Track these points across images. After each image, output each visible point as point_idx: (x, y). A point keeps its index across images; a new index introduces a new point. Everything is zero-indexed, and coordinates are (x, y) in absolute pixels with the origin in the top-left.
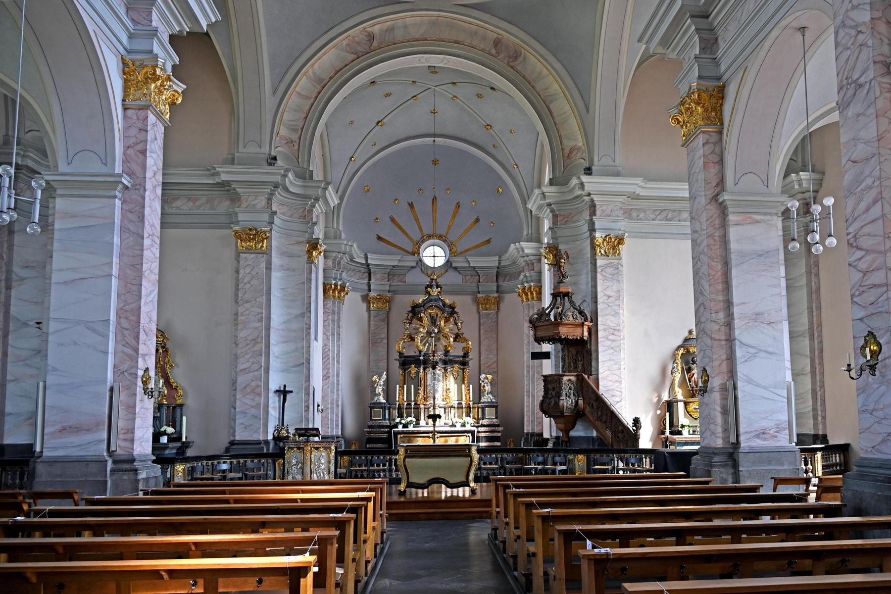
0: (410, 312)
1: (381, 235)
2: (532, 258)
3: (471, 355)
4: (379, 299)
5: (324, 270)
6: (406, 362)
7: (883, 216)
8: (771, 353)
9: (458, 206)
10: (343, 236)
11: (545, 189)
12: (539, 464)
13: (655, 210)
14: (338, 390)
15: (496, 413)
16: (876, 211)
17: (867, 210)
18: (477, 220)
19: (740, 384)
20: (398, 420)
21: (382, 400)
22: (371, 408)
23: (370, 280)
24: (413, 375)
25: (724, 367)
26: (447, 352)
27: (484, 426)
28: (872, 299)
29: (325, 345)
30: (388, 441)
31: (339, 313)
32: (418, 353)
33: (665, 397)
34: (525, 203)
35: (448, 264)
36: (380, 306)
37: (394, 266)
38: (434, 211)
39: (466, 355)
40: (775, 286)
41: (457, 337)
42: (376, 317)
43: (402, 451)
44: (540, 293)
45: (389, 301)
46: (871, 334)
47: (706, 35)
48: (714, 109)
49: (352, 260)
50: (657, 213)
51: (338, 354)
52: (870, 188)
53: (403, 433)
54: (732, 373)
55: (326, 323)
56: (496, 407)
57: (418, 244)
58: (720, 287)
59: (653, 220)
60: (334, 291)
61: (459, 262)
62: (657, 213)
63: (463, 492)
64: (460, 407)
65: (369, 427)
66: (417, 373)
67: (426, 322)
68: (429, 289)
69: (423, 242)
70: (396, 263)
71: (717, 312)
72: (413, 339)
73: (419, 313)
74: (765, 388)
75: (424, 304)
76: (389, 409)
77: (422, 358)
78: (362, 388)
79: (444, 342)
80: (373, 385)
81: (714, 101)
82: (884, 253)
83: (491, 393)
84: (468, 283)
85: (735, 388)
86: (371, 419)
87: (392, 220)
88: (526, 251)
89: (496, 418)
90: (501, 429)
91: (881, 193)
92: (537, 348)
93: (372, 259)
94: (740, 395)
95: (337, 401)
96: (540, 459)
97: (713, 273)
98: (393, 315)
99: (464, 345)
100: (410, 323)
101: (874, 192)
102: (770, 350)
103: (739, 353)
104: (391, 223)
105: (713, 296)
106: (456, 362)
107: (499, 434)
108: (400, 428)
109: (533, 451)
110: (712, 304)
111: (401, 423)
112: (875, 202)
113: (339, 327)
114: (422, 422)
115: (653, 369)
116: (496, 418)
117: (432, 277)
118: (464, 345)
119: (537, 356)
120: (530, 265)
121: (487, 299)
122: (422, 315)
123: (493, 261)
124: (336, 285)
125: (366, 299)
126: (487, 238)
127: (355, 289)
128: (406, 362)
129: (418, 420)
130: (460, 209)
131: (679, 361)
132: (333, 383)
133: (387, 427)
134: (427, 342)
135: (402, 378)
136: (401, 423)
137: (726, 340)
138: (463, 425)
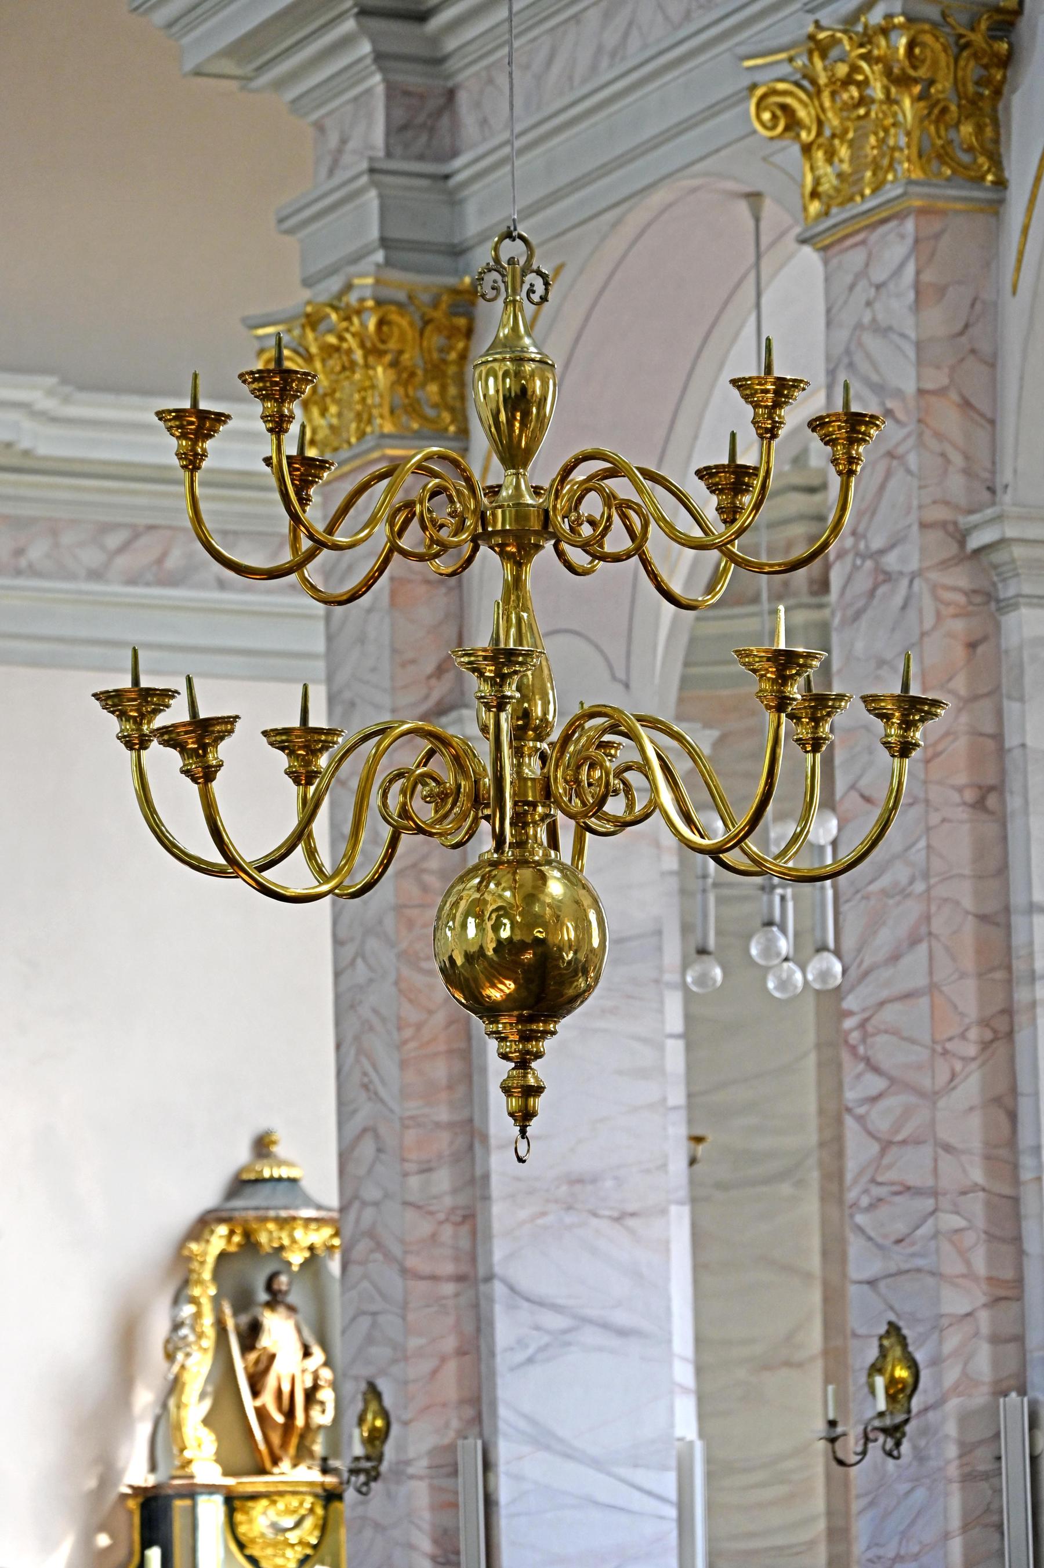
7: (933, 988)
8: (623, 1333)
13: (106, 528)
16: (913, 970)
17: (895, 958)
19: (504, 1451)
25: (449, 1386)
28: (900, 1228)
33: (136, 1473)
40: (642, 1073)
46: (894, 1329)
47: (413, 79)
48: (436, 371)
50: (113, 541)
52: (904, 893)
54: (478, 1408)
58: (440, 1071)
59: (95, 575)
62: (113, 541)
71: (426, 1169)
74: (596, 1464)
81: (435, 340)
82: (932, 1097)
85: (488, 1466)
91: (928, 918)
94: (504, 1494)
97: (413, 1015)
101: (913, 909)
102: (621, 1318)
103: (507, 1329)
105: (413, 1107)
110: (411, 1136)
112: (914, 941)
115: (72, 1329)
131: (206, 1291)
137: (460, 1278)
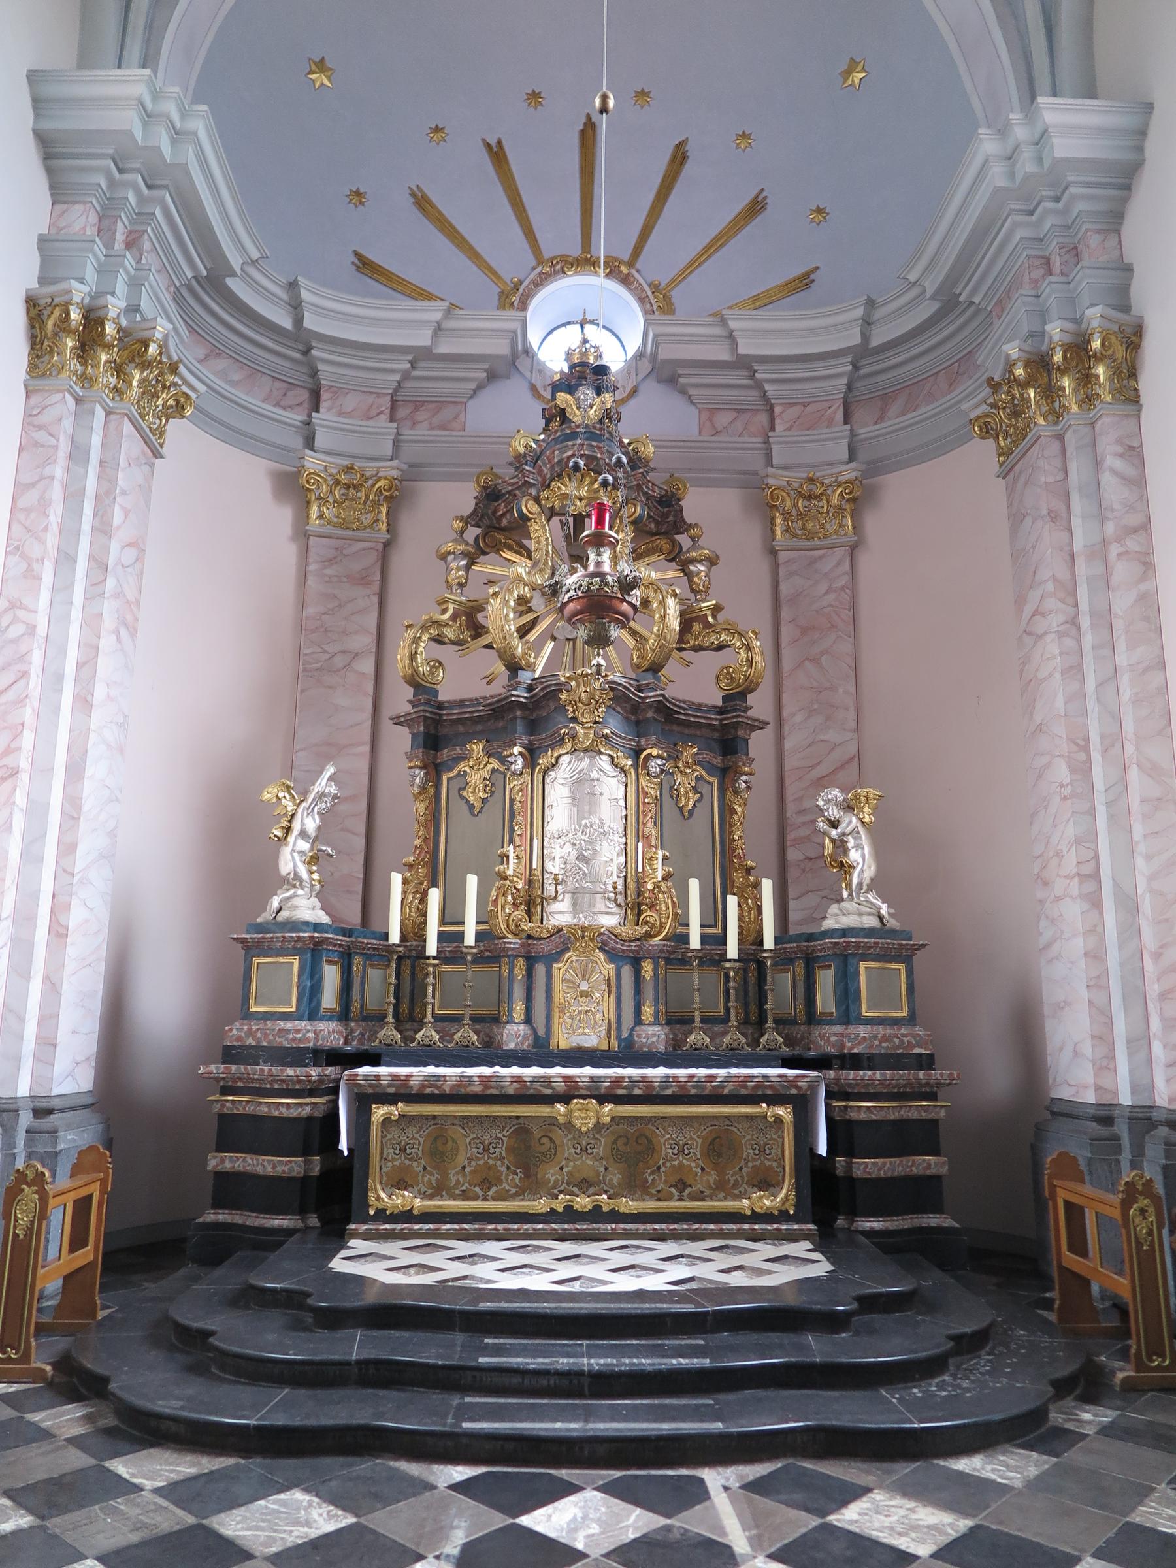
6: (439, 733)
9: (679, 157)
18: (756, 207)
36: (350, 522)
37: (420, 356)
39: (736, 698)
42: (331, 561)
51: (87, 664)
55: (30, 499)
70: (423, 339)
83: (875, 885)
87: (422, 202)
93: (320, 311)
125: (293, 487)
128: (439, 733)
130: (689, 169)
132: (37, 811)
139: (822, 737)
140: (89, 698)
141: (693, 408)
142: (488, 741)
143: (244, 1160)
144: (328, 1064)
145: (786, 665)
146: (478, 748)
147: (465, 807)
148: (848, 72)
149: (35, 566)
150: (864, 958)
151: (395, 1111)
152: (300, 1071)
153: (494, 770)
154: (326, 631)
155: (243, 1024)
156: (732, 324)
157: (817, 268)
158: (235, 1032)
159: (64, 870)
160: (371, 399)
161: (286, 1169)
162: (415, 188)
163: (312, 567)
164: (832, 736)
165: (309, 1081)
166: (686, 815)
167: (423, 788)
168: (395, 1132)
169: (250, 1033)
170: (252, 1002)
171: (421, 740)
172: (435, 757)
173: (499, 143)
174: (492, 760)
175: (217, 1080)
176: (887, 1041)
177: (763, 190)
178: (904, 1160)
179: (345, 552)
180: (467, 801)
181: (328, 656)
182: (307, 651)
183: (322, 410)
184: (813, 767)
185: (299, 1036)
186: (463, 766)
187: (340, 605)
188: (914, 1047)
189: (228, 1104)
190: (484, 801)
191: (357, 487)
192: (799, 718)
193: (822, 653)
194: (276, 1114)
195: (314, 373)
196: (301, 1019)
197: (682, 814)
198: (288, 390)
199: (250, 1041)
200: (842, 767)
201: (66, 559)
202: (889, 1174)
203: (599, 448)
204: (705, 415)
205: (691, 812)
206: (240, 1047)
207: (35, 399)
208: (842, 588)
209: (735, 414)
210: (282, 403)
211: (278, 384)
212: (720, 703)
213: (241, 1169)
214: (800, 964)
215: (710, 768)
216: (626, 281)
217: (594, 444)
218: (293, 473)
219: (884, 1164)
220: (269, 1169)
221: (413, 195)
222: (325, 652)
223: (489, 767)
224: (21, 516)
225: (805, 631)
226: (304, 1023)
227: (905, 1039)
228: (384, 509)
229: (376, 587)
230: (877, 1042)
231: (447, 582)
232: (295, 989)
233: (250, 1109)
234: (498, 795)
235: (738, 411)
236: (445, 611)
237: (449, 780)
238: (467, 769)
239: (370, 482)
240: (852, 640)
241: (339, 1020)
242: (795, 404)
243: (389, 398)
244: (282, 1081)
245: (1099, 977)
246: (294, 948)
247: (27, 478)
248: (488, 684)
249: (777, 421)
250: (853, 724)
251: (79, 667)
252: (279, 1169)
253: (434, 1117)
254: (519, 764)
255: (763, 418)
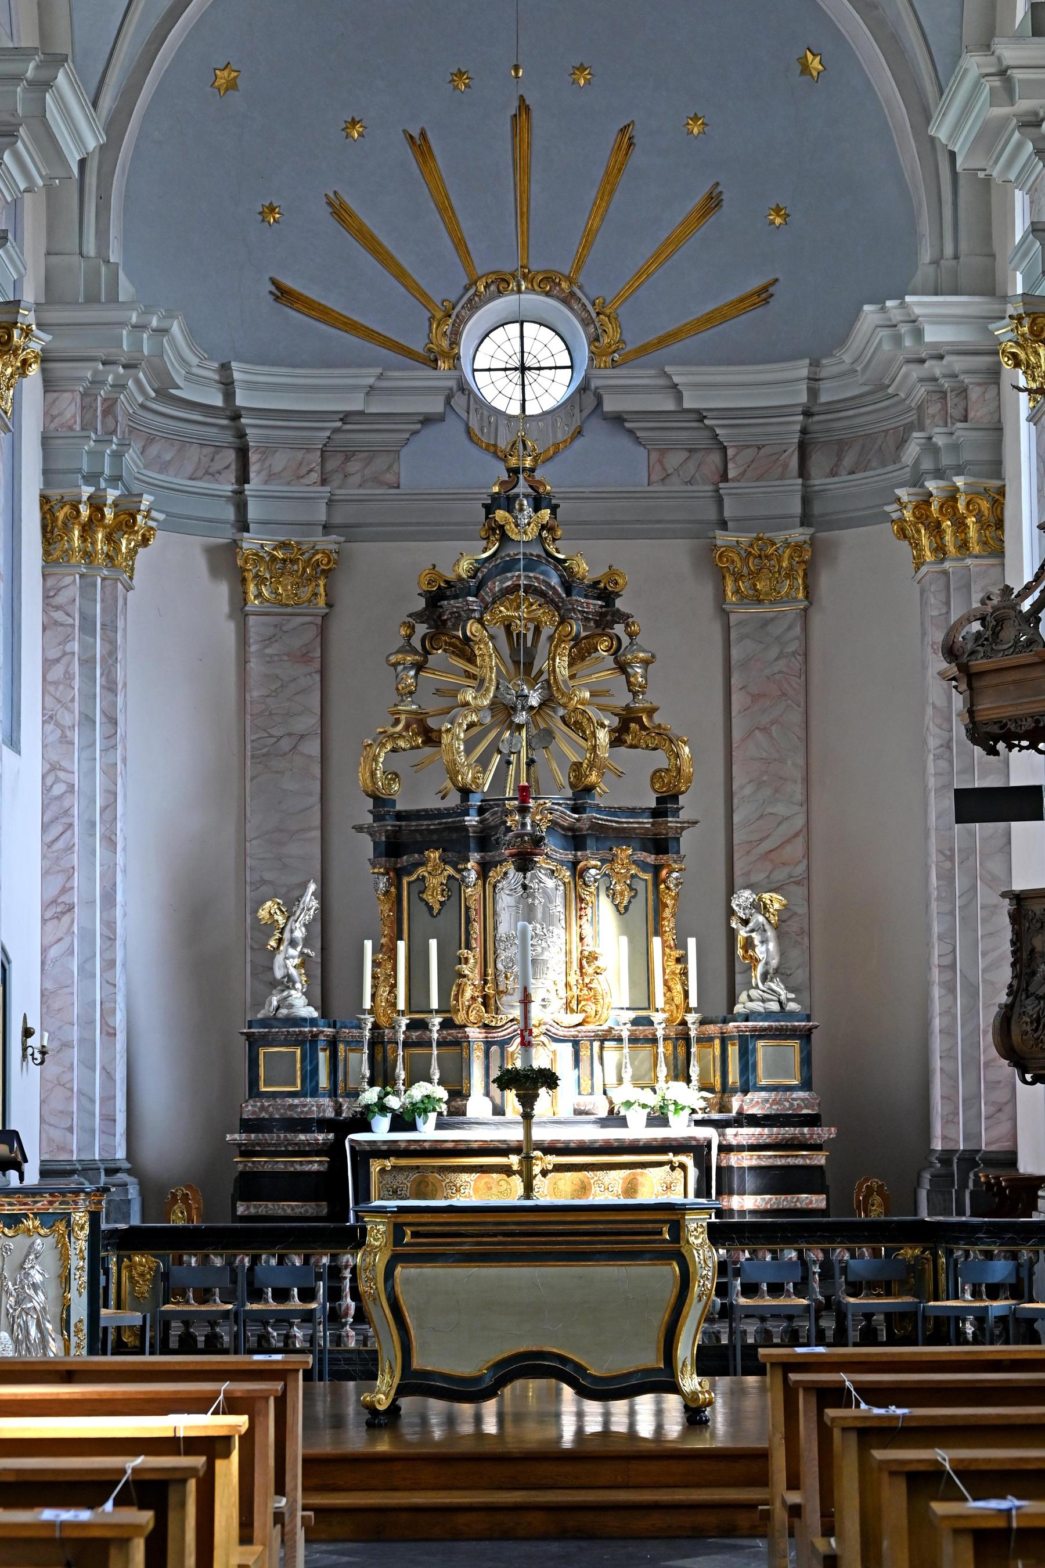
0: (419, 616)
1: (289, 282)
2: (958, 363)
3: (688, 806)
4: (284, 562)
5: (46, 440)
10: (126, 289)
11: (1009, 53)
12: (994, 1292)
14: (110, 964)
15: (806, 1061)
18: (713, 202)
20: (371, 1095)
21: (303, 1008)
22: (254, 1042)
23: (243, 478)
24: (434, 898)
26: (581, 795)
27: (753, 1121)
29: (52, 769)
30: (328, 1187)
31: (110, 627)
32: (454, 800)
34: (923, 115)
35: (585, 397)
36: (286, 590)
38: (521, 165)
39: (666, 804)
41: (627, 726)
42: (270, 640)
43: (378, 1233)
44: (995, 523)
45: (328, 572)
49: (163, 395)
51: (110, 806)
53: (391, 1150)
56: (805, 1036)
57: (453, 317)
60: (87, 530)
61: (634, 392)
63: (648, 1417)
64: (642, 1036)
65: (247, 1126)
66: (454, 886)
67: (491, 659)
68: (500, 515)
69: (473, 307)
72: (431, 738)
73: (460, 619)
75: (477, 583)
76: (333, 1044)
77: (472, 820)
78: (211, 950)
79: (568, 748)
80: (262, 939)
84: (676, 486)
86: (254, 1091)
87: (339, 211)
88: (932, 335)
89: (806, 1084)
90: (825, 1133)
92: (984, 773)
93: (251, 386)
95: (108, 1013)
96: (1000, 1270)
98: (345, 628)
99: (660, 759)
100: (419, 667)
104: (333, 224)
106: (623, 836)
107: (820, 1159)
108: (381, 1130)
109: (966, 1233)
111: (383, 1109)
113: (111, 687)
114: (478, 1105)
116: (806, 1084)
117: (517, 466)
118: (660, 759)
119: (978, 805)
120: (951, 398)
121: (760, 556)
122: (472, 628)
123: (782, 385)
124: (97, 506)
125: (227, 562)
126: (756, 283)
127: (175, 523)
129: (458, 1094)
132: (87, 935)
133: (324, 1125)
134: (494, 748)
135: (385, 909)
136: (383, 1109)
138: (658, 1118)
139: (771, 811)
140: (113, 837)
141: (642, 448)
142: (444, 850)
143: (266, 1206)
144: (329, 1132)
145: (736, 735)
146: (434, 855)
147: (425, 908)
148: (805, 69)
149: (68, 733)
150: (760, 1037)
151: (388, 1164)
152: (309, 1136)
153: (450, 877)
154: (271, 714)
155: (255, 1102)
156: (676, 379)
157: (776, 280)
158: (250, 1108)
159: (108, 982)
160: (300, 455)
161: (302, 1211)
162: (332, 195)
163: (253, 648)
164: (780, 809)
165: (318, 1144)
166: (622, 911)
167: (387, 893)
168: (388, 1178)
169: (263, 1108)
170: (262, 1083)
171: (383, 848)
172: (396, 863)
173: (423, 134)
174: (448, 867)
175: (240, 1145)
176: (777, 1104)
177: (718, 184)
178: (789, 1197)
179: (284, 628)
180: (427, 904)
181: (275, 739)
182: (254, 737)
183: (252, 475)
184: (762, 840)
185: (305, 1109)
186: (421, 871)
187: (282, 686)
188: (802, 1109)
189: (249, 1164)
190: (442, 903)
191: (294, 561)
192: (747, 791)
193: (773, 723)
194: (292, 1169)
195: (241, 435)
196: (305, 1096)
197: (618, 911)
198: (216, 453)
199: (263, 1115)
200: (789, 841)
201: (88, 720)
202: (775, 1207)
203: (536, 578)
204: (654, 456)
205: (626, 908)
206: (256, 1119)
207: (50, 582)
208: (794, 654)
209: (687, 454)
210: (211, 470)
211: (206, 450)
212: (653, 805)
213: (264, 1213)
214: (717, 1042)
215: (643, 866)
216: (568, 300)
217: (531, 575)
218: (227, 545)
219: (771, 1199)
220: (289, 1211)
221: (330, 204)
222: (271, 736)
223: (446, 873)
224: (51, 689)
225: (755, 698)
226: (309, 1099)
227: (795, 1103)
228: (321, 583)
229: (317, 665)
230: (768, 1105)
231: (397, 689)
232: (299, 1073)
233: (268, 1168)
234: (454, 899)
235: (690, 450)
236: (397, 722)
237: (409, 883)
238: (426, 874)
239: (306, 556)
240: (802, 709)
241: (330, 1097)
242: (748, 447)
243: (319, 453)
244: (296, 1144)
245: (949, 1050)
246: (296, 1040)
247: (53, 654)
248: (443, 798)
249: (730, 465)
250: (799, 797)
251: (103, 810)
252: (297, 1210)
253: (418, 1167)
254: (473, 876)
255: (715, 458)
